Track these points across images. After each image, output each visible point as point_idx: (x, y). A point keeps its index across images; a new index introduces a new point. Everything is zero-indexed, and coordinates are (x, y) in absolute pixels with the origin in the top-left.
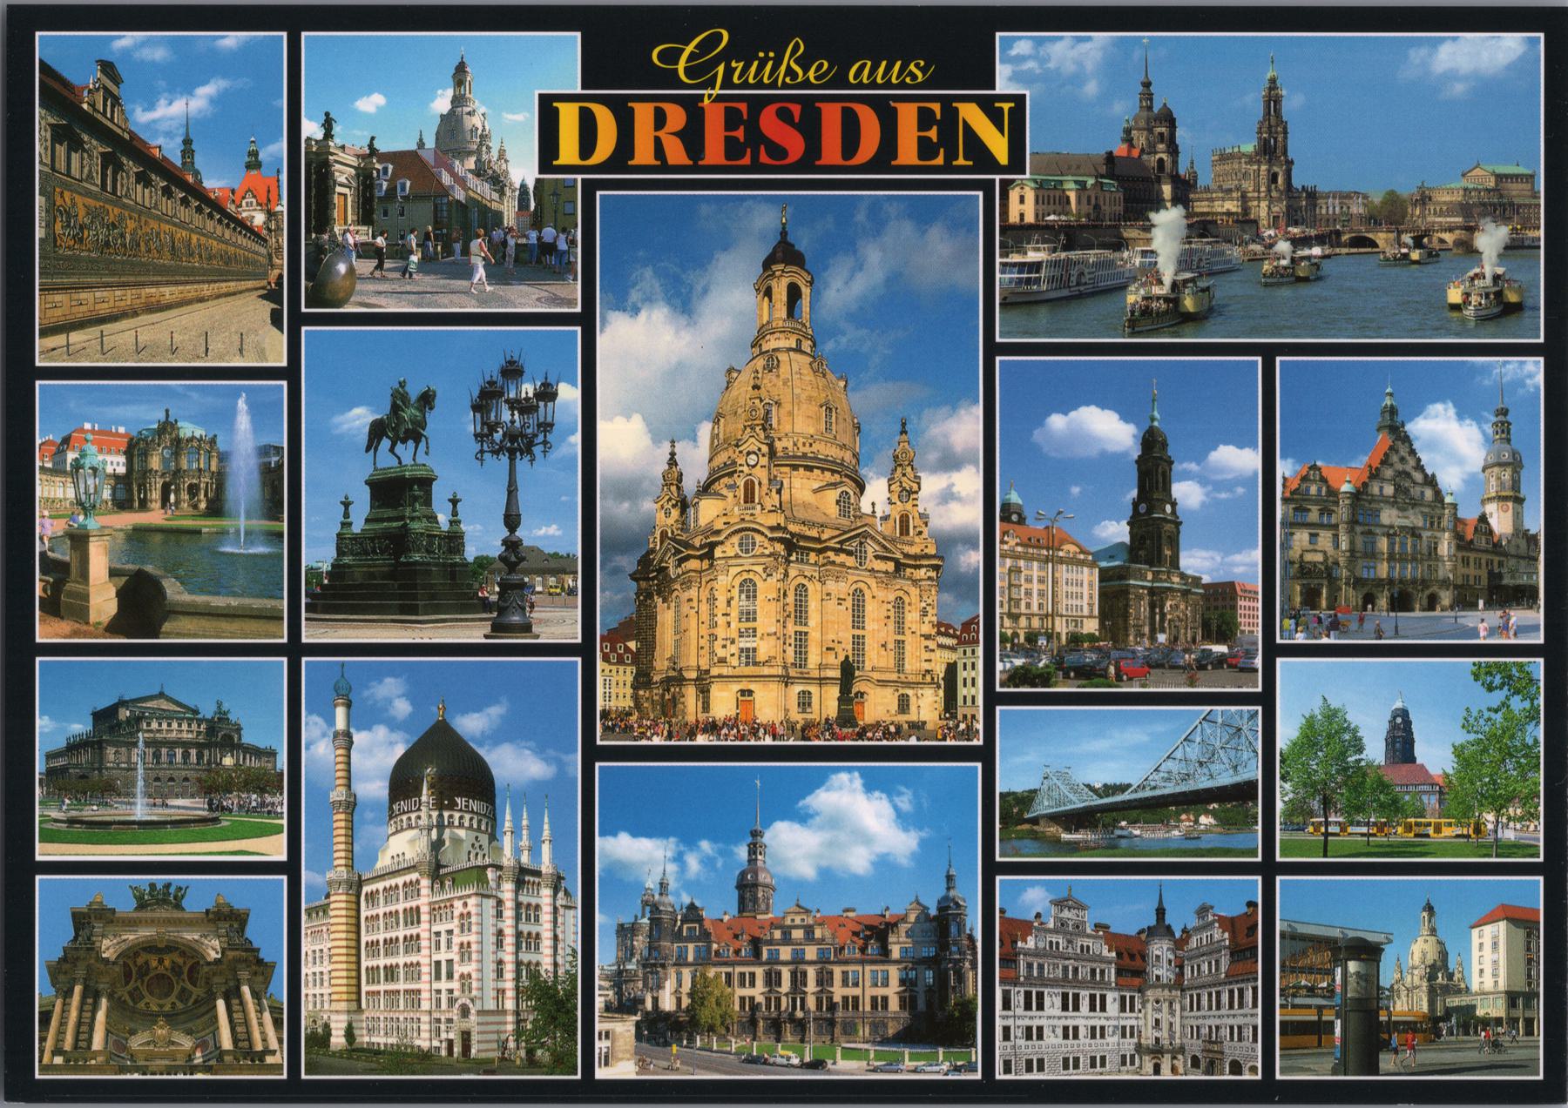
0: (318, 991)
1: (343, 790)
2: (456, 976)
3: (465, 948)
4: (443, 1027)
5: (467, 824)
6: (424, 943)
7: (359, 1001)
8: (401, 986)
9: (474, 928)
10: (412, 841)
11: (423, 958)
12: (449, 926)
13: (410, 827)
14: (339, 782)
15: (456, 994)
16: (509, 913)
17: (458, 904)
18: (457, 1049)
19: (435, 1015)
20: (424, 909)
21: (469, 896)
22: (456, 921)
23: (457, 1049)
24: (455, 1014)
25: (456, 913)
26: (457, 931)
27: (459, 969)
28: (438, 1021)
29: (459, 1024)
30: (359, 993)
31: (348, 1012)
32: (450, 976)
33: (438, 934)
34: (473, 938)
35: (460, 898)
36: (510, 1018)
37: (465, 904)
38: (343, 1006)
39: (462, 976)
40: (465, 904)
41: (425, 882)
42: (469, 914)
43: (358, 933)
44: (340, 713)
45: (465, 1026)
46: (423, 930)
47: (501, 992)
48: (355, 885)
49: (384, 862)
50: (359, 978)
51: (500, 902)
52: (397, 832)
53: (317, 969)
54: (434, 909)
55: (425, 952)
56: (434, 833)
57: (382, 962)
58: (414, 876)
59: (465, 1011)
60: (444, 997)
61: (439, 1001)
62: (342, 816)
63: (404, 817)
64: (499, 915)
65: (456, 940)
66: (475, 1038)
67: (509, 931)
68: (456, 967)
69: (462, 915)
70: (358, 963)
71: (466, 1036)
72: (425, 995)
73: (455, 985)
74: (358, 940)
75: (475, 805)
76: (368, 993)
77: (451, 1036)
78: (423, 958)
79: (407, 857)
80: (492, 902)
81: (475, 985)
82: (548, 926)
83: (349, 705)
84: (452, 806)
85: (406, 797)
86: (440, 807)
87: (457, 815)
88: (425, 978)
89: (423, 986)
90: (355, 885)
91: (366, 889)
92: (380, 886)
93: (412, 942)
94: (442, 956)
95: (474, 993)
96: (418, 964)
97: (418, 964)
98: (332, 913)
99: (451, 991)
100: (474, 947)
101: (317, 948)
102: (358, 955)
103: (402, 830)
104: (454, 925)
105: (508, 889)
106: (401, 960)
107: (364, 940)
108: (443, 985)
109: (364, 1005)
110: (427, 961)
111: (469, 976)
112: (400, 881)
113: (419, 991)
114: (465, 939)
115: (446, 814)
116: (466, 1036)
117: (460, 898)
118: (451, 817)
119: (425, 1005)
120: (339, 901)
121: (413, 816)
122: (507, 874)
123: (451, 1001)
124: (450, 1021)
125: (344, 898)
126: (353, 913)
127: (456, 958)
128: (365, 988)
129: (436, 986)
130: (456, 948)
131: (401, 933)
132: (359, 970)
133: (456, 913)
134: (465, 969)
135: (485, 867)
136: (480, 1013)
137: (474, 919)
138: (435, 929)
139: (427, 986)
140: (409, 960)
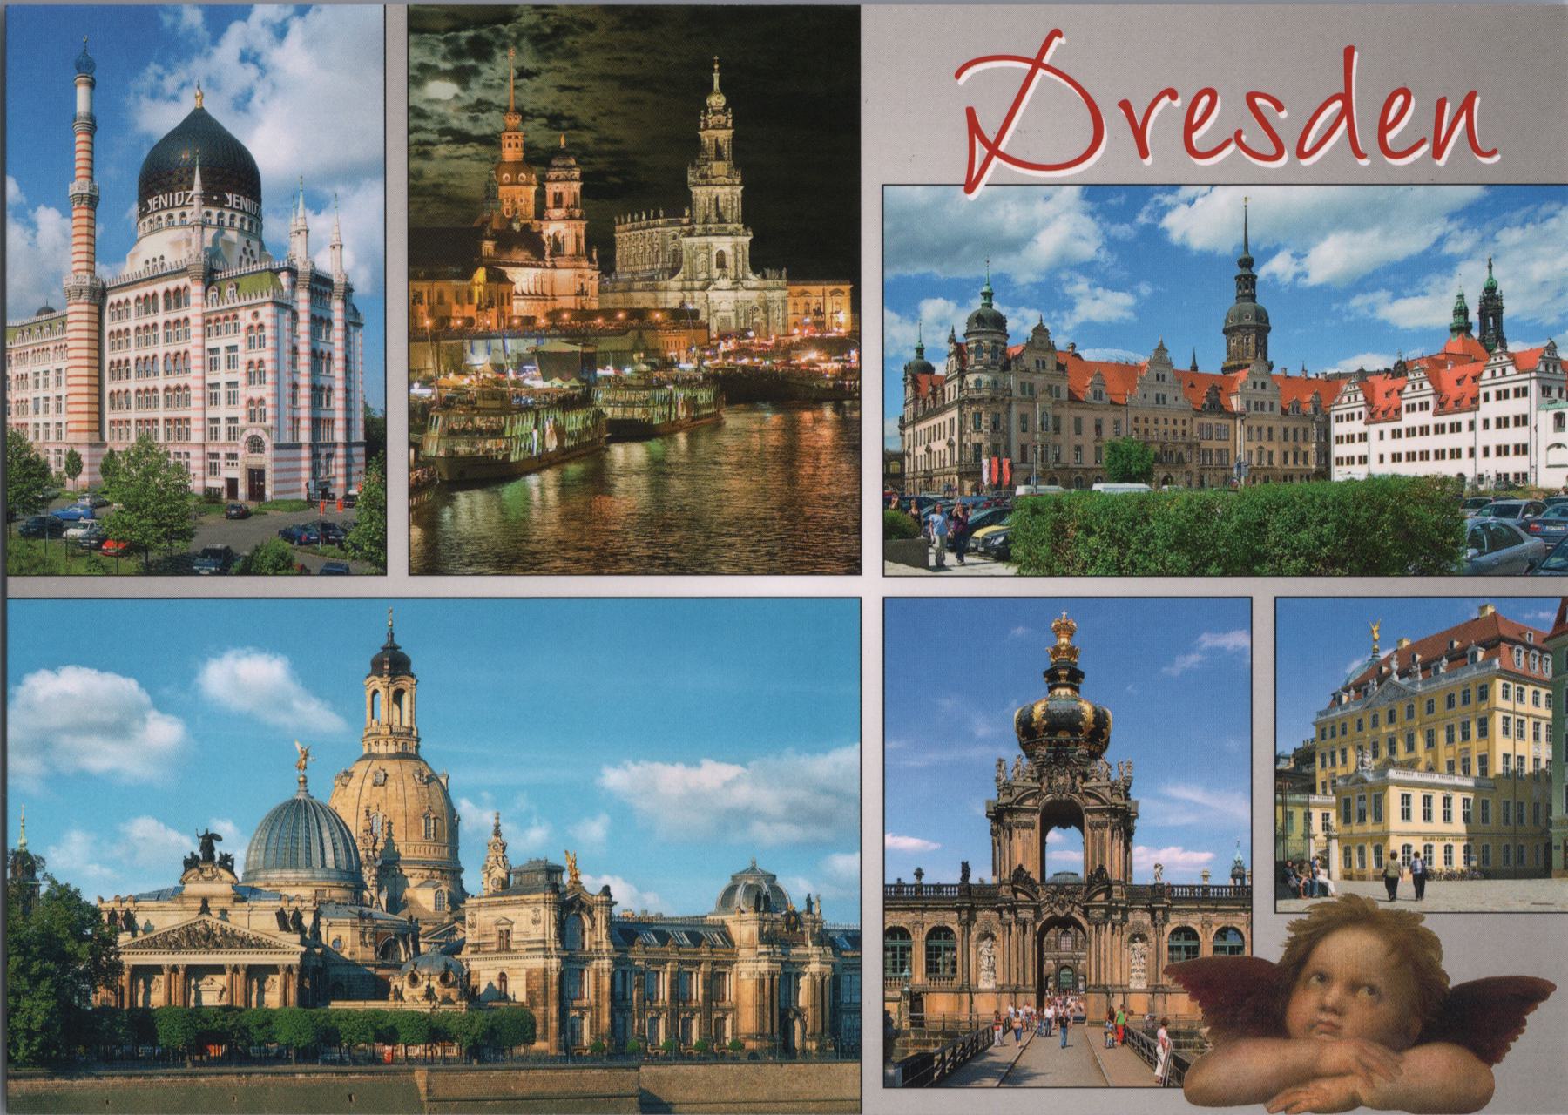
0: (41, 419)
1: (87, 181)
2: (242, 402)
3: (255, 372)
4: (222, 462)
5: (237, 224)
6: (195, 362)
7: (101, 431)
8: (161, 413)
9: (269, 343)
10: (175, 244)
11: (193, 379)
12: (231, 342)
13: (171, 226)
14: (79, 173)
15: (242, 423)
16: (303, 327)
17: (245, 318)
18: (242, 490)
19: (211, 449)
20: (196, 321)
21: (263, 304)
22: (242, 335)
23: (242, 490)
24: (241, 448)
25: (243, 326)
26: (242, 347)
27: (245, 392)
28: (216, 456)
29: (246, 459)
30: (100, 422)
31: (91, 445)
32: (232, 399)
33: (215, 351)
34: (267, 355)
35: (249, 307)
36: (305, 453)
37: (256, 315)
38: (84, 437)
39: (251, 401)
40: (256, 315)
41: (196, 289)
42: (261, 326)
43: (100, 350)
44: (82, 93)
45: (256, 460)
46: (193, 345)
47: (296, 421)
48: (98, 295)
49: (134, 266)
50: (100, 404)
51: (295, 315)
52: (152, 232)
53: (41, 394)
54: (210, 324)
55: (196, 372)
56: (210, 233)
57: (133, 384)
58: (181, 282)
59: (256, 445)
60: (223, 426)
61: (214, 434)
62: (85, 213)
63: (164, 214)
64: (293, 329)
65: (243, 357)
66: (269, 476)
67: (304, 349)
68: (241, 390)
69: (250, 327)
70: (100, 386)
71: (256, 475)
72: (196, 425)
73: (240, 412)
74: (100, 359)
75: (246, 203)
76: (112, 422)
77: (232, 474)
78: (193, 379)
79: (166, 261)
80: (288, 314)
81: (269, 412)
82: (339, 344)
83: (92, 85)
84: (221, 203)
85: (169, 189)
86: (207, 200)
87: (227, 214)
88: (196, 403)
89: (194, 412)
90: (98, 295)
91: (112, 298)
92: (131, 295)
93: (178, 362)
94: (222, 376)
95: (269, 422)
96: (187, 387)
97: (187, 387)
98: (70, 326)
99: (233, 420)
100: (269, 367)
101: (41, 369)
102: (100, 377)
103: (160, 228)
104: (239, 340)
105: (303, 295)
106: (160, 382)
107: (109, 356)
108: (222, 411)
109: (107, 438)
110: (199, 383)
111: (261, 401)
112: (160, 288)
113: (188, 420)
114: (255, 357)
115: (215, 212)
116: (256, 475)
117: (249, 307)
118: (220, 215)
119: (196, 437)
120: (78, 313)
121: (176, 213)
122: (304, 278)
123: (232, 434)
124: (232, 456)
125: (85, 308)
126: (96, 327)
127: (242, 380)
128: (109, 416)
129: (211, 414)
130: (242, 368)
131: (160, 349)
132: (100, 395)
133: (243, 326)
134: (255, 392)
135: (278, 272)
136: (277, 447)
137: (268, 332)
138: (210, 344)
139: (199, 414)
140: (143, 384)
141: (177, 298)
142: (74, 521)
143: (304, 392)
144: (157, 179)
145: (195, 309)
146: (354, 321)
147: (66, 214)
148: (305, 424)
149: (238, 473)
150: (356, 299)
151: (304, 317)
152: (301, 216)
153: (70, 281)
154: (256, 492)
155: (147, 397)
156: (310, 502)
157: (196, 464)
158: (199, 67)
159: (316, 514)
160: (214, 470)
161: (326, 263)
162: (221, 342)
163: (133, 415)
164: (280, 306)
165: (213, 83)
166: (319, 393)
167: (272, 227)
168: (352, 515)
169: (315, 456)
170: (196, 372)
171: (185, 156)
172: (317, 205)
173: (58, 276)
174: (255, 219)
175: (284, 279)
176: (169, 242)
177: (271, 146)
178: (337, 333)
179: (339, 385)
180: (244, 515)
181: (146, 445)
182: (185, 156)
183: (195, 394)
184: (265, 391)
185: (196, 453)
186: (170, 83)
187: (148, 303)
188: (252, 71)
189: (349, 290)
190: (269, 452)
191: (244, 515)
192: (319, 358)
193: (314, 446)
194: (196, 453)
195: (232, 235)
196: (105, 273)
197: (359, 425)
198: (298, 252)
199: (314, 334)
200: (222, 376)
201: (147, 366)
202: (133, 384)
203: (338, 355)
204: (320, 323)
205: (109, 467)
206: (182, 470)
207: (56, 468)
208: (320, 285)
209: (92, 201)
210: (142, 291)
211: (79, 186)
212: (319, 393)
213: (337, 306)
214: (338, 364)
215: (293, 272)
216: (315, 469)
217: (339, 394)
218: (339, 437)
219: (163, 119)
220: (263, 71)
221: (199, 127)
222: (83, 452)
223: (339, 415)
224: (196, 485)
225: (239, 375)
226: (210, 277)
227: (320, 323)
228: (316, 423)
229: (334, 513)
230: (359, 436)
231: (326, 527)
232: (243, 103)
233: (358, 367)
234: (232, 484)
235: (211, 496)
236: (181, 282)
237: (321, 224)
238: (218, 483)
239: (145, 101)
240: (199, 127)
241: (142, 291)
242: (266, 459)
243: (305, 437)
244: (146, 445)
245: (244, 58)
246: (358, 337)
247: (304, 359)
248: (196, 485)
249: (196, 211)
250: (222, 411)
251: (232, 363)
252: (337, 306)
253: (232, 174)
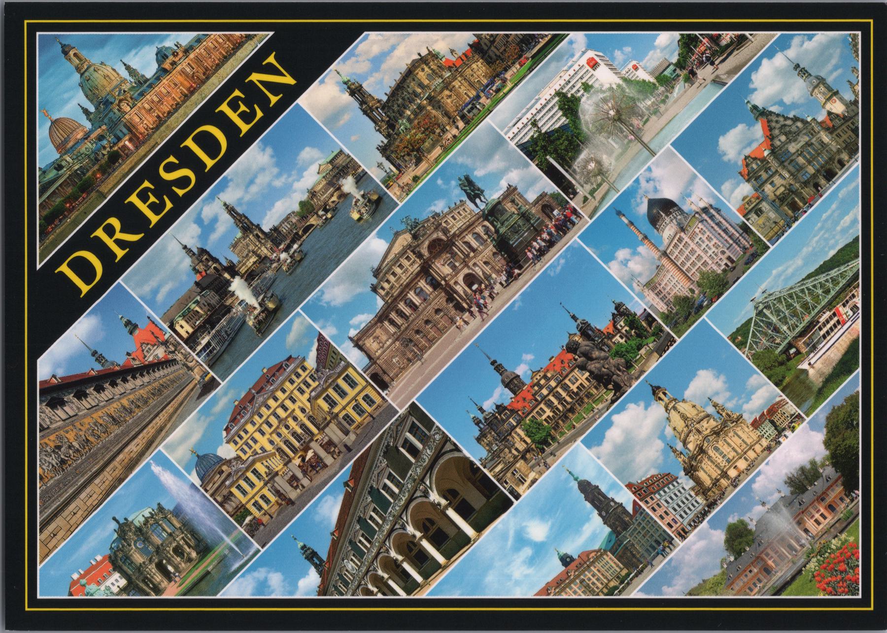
8: (699, 264)
16: (709, 221)
17: (697, 230)
18: (729, 264)
23: (729, 264)
24: (721, 256)
27: (711, 245)
29: (724, 257)
32: (710, 248)
34: (708, 233)
41: (682, 234)
45: (726, 255)
48: (665, 254)
55: (698, 250)
56: (674, 221)
57: (688, 264)
58: (678, 236)
59: (723, 253)
65: (704, 238)
67: (713, 225)
71: (729, 258)
72: (708, 260)
73: (714, 249)
75: (675, 208)
84: (671, 213)
86: (668, 215)
89: (705, 258)
90: (665, 254)
91: (668, 252)
92: (671, 247)
93: (693, 252)
94: (704, 246)
104: (700, 236)
106: (693, 258)
107: (678, 264)
108: (710, 252)
112: (675, 241)
114: (706, 236)
116: (729, 258)
119: (710, 262)
120: (664, 261)
122: (701, 212)
123: (716, 255)
131: (687, 252)
134: (713, 243)
141: (680, 240)
142: (703, 301)
143: (722, 233)
144: (654, 221)
145: (686, 239)
146: (718, 211)
147: (643, 245)
148: (729, 239)
149: (725, 261)
150: (714, 206)
151: (708, 219)
152: (688, 201)
153: (657, 257)
154: (732, 261)
155: (693, 264)
156: (745, 253)
157: (715, 267)
158: (641, 192)
159: (748, 255)
160: (720, 265)
161: (702, 205)
162: (697, 240)
163: (694, 270)
164: (701, 221)
165: (646, 192)
166: (725, 231)
167: (685, 208)
168: (754, 248)
169: (737, 243)
170: (698, 250)
171: (655, 211)
172: (689, 195)
173: (654, 258)
174: (680, 209)
175: (697, 216)
176: (669, 230)
177: (669, 193)
178: (717, 216)
179: (727, 225)
180: (734, 268)
181: (703, 274)
182: (655, 211)
183: (702, 254)
184: (715, 240)
185: (713, 265)
186: (638, 200)
187: (676, 246)
188: (651, 182)
189: (711, 206)
190: (727, 251)
191: (734, 268)
192: (719, 224)
193: (735, 242)
194: (713, 265)
195: (679, 217)
196: (662, 248)
197: (739, 229)
198: (694, 208)
199: (713, 220)
200: (704, 246)
201: (688, 258)
202: (688, 264)
203: (722, 220)
204: (712, 217)
205: (699, 285)
206: (713, 271)
207: (689, 295)
208: (705, 210)
209: (646, 237)
210: (672, 245)
211: (641, 237)
212: (725, 231)
213: (712, 211)
214: (723, 221)
215: (697, 213)
216: (739, 246)
217: (729, 227)
218: (738, 235)
219: (644, 208)
220: (654, 180)
221: (652, 203)
222: (691, 286)
223: (733, 231)
224: (719, 272)
225: (707, 242)
226: (683, 229)
227: (712, 217)
228: (730, 237)
229: (751, 251)
230: (741, 231)
231: (752, 255)
232: (656, 190)
233: (728, 219)
234: (726, 264)
235: (724, 271)
236: (678, 236)
237: (694, 198)
238: (723, 267)
239: (638, 209)
240: (652, 203)
241: (672, 245)
242: (728, 253)
243: (731, 242)
244: (703, 274)
245: (648, 182)
246: (722, 213)
247: (716, 227)
248: (719, 272)
249: (667, 220)
250: (710, 252)
251: (703, 242)
252: (712, 211)
253: (667, 206)
